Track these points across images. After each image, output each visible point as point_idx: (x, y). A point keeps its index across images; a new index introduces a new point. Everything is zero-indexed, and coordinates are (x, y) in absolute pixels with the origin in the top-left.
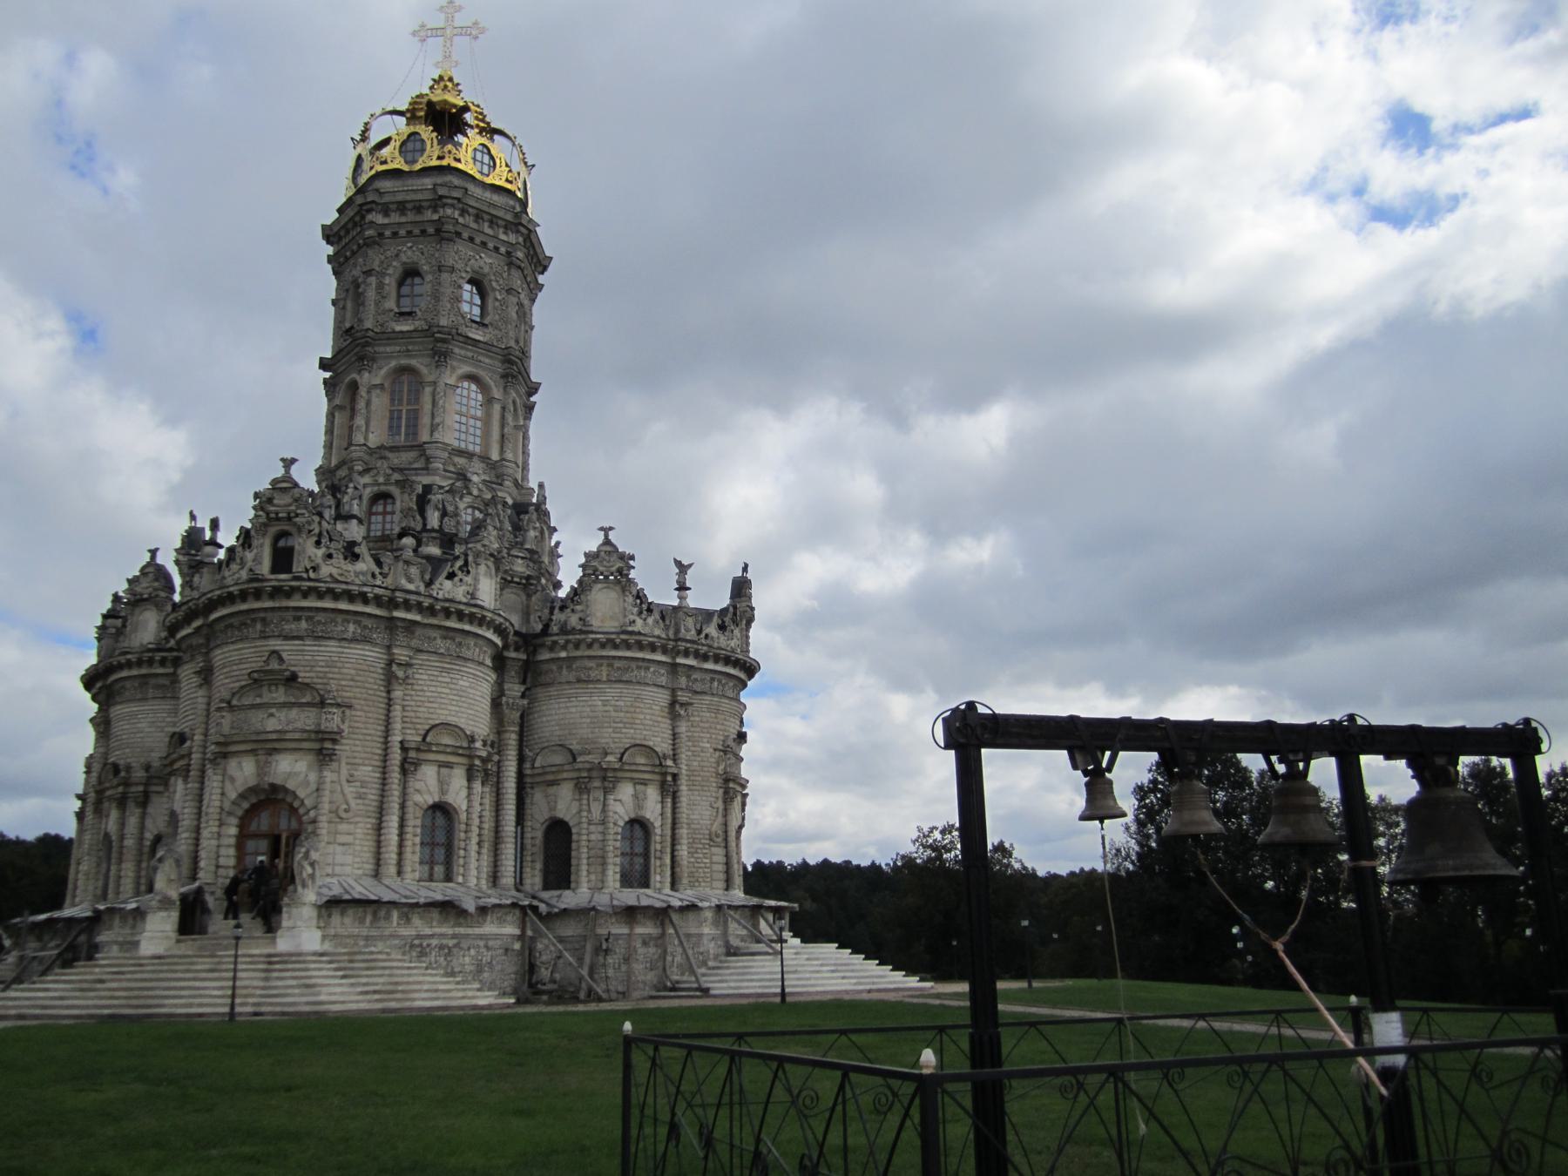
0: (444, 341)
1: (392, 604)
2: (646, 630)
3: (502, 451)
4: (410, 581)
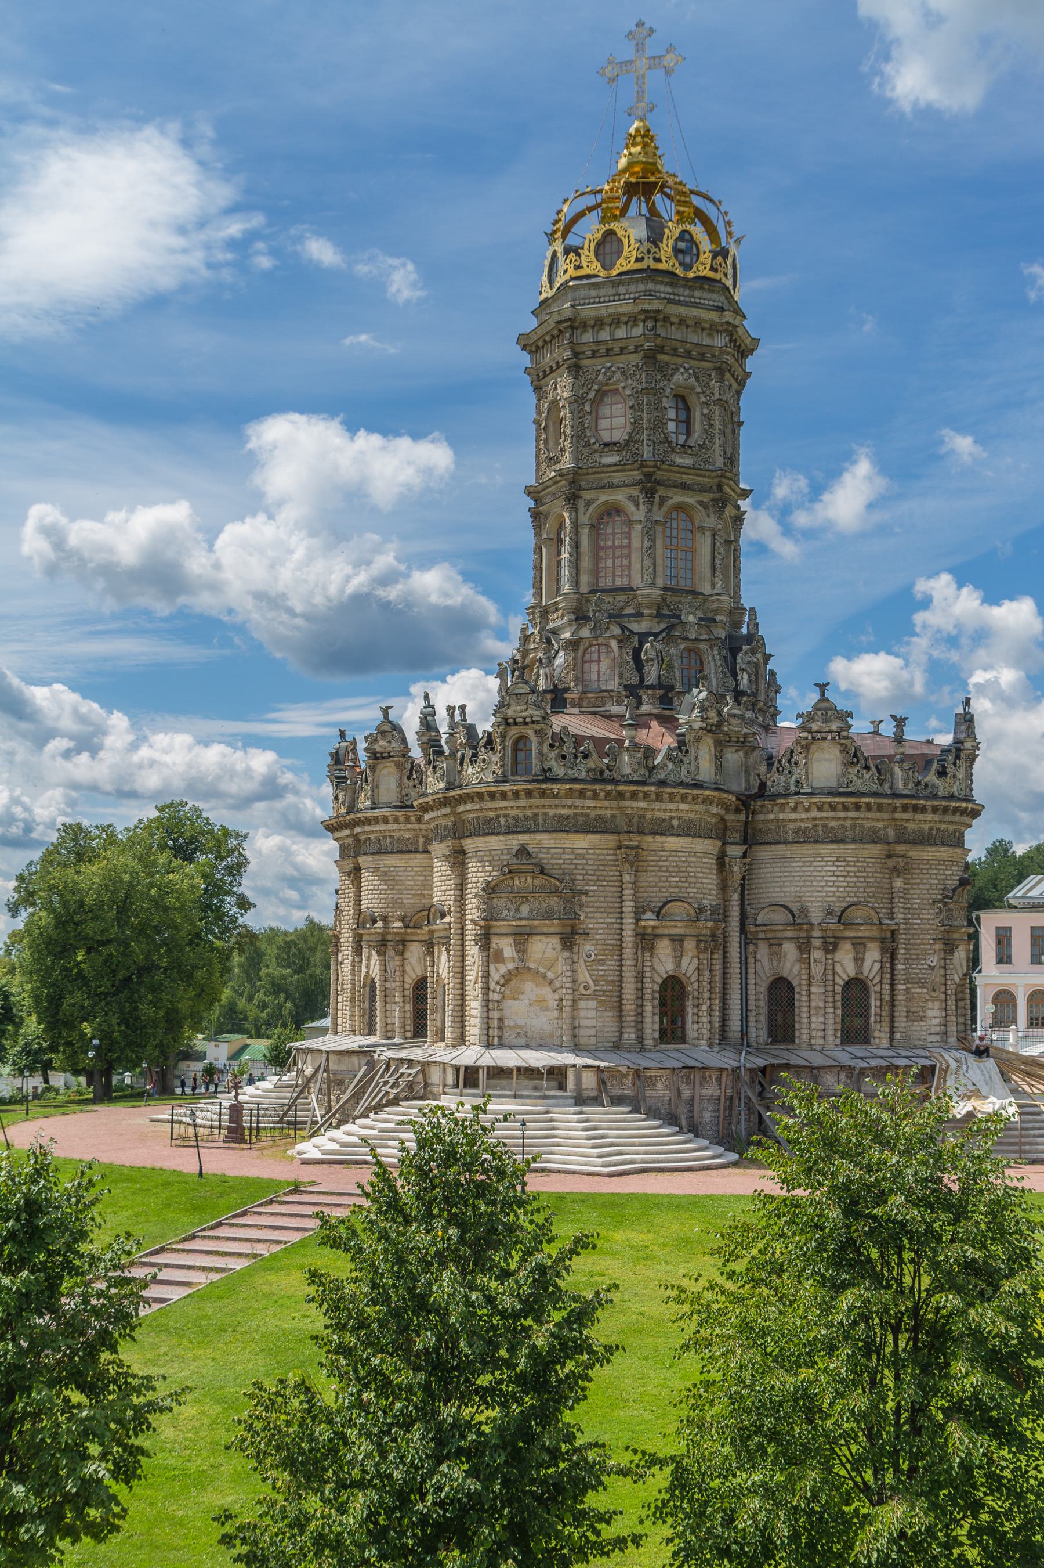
1: (621, 796)
3: (713, 585)
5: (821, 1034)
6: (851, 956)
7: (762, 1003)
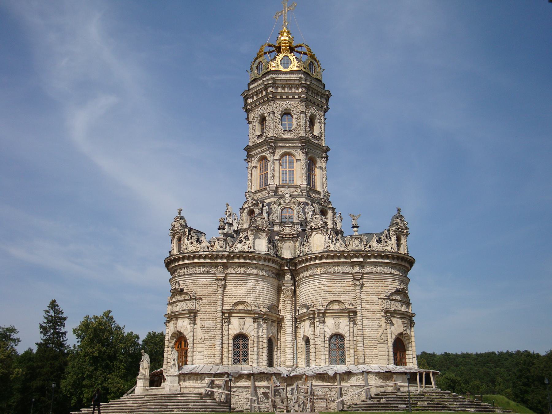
0: (271, 142)
2: (336, 249)
4: (221, 247)
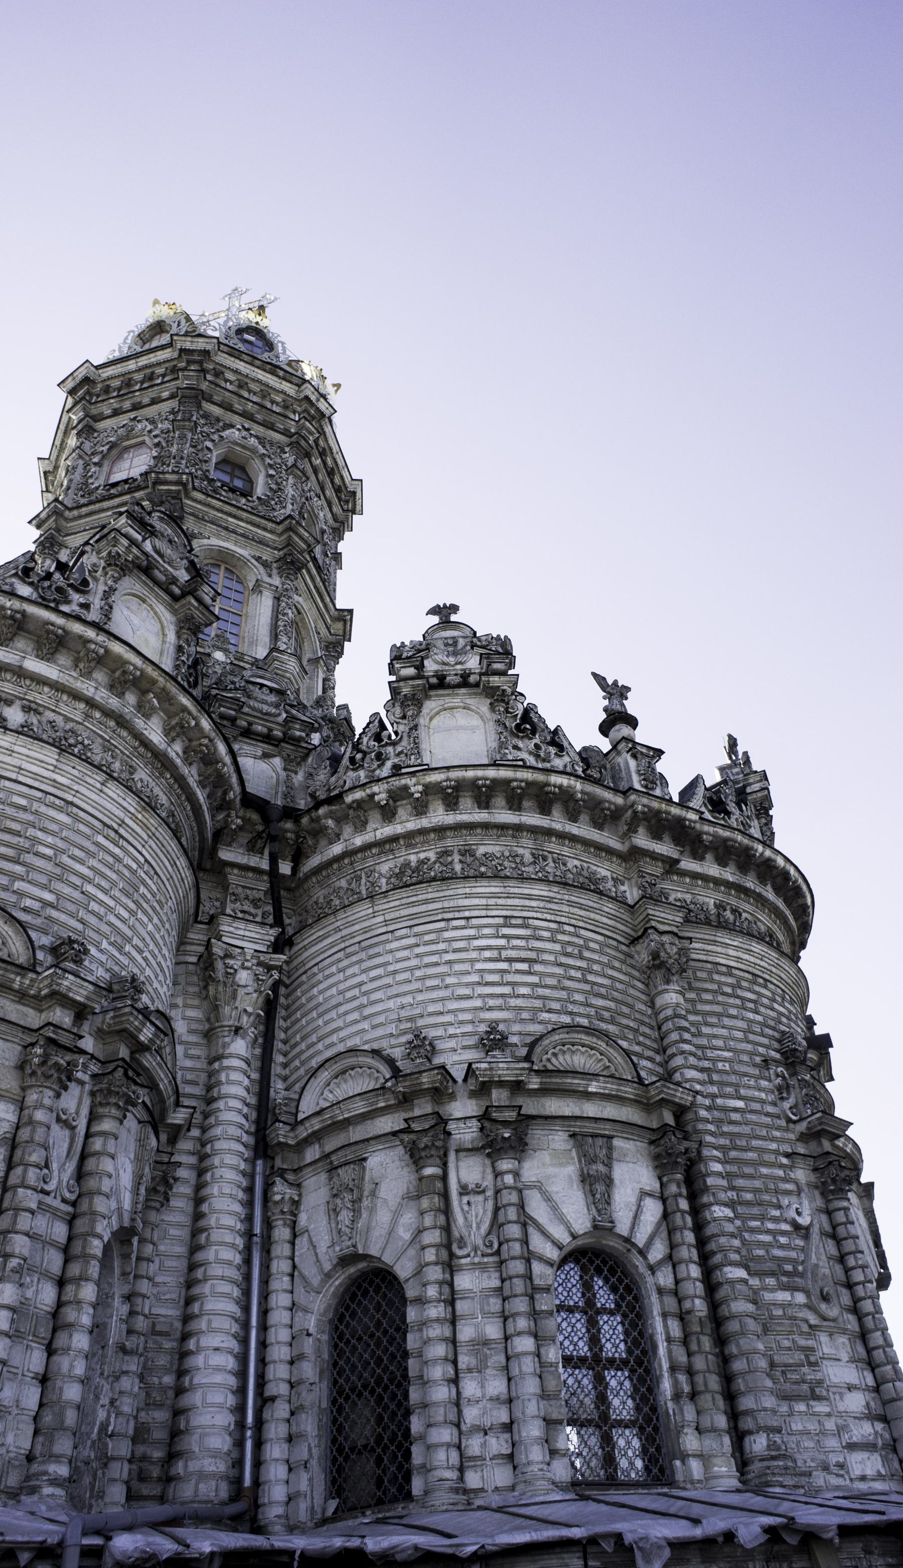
5: (498, 1444)
6: (571, 1170)
7: (308, 1370)
